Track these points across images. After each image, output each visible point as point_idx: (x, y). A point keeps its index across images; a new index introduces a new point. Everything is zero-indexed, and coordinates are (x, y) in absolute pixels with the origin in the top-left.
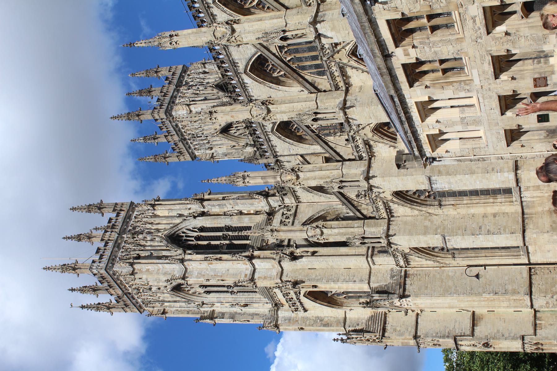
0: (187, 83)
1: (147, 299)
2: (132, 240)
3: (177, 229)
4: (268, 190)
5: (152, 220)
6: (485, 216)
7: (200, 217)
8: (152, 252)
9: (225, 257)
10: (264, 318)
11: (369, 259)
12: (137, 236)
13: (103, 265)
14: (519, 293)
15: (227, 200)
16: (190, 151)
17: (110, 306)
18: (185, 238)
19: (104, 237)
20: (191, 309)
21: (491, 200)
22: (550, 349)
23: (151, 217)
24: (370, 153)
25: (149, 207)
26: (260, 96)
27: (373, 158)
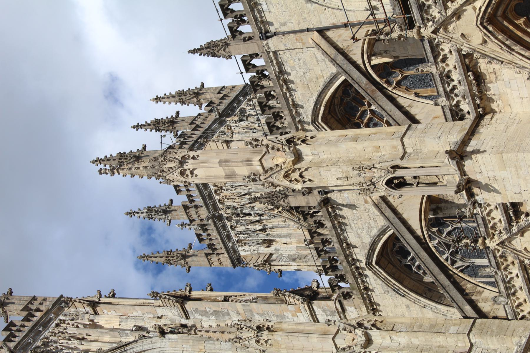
0: (243, 111)
4: (318, 287)
5: (83, 332)
15: (232, 301)
16: (230, 245)
24: (481, 99)
26: (285, 24)
27: (488, 117)
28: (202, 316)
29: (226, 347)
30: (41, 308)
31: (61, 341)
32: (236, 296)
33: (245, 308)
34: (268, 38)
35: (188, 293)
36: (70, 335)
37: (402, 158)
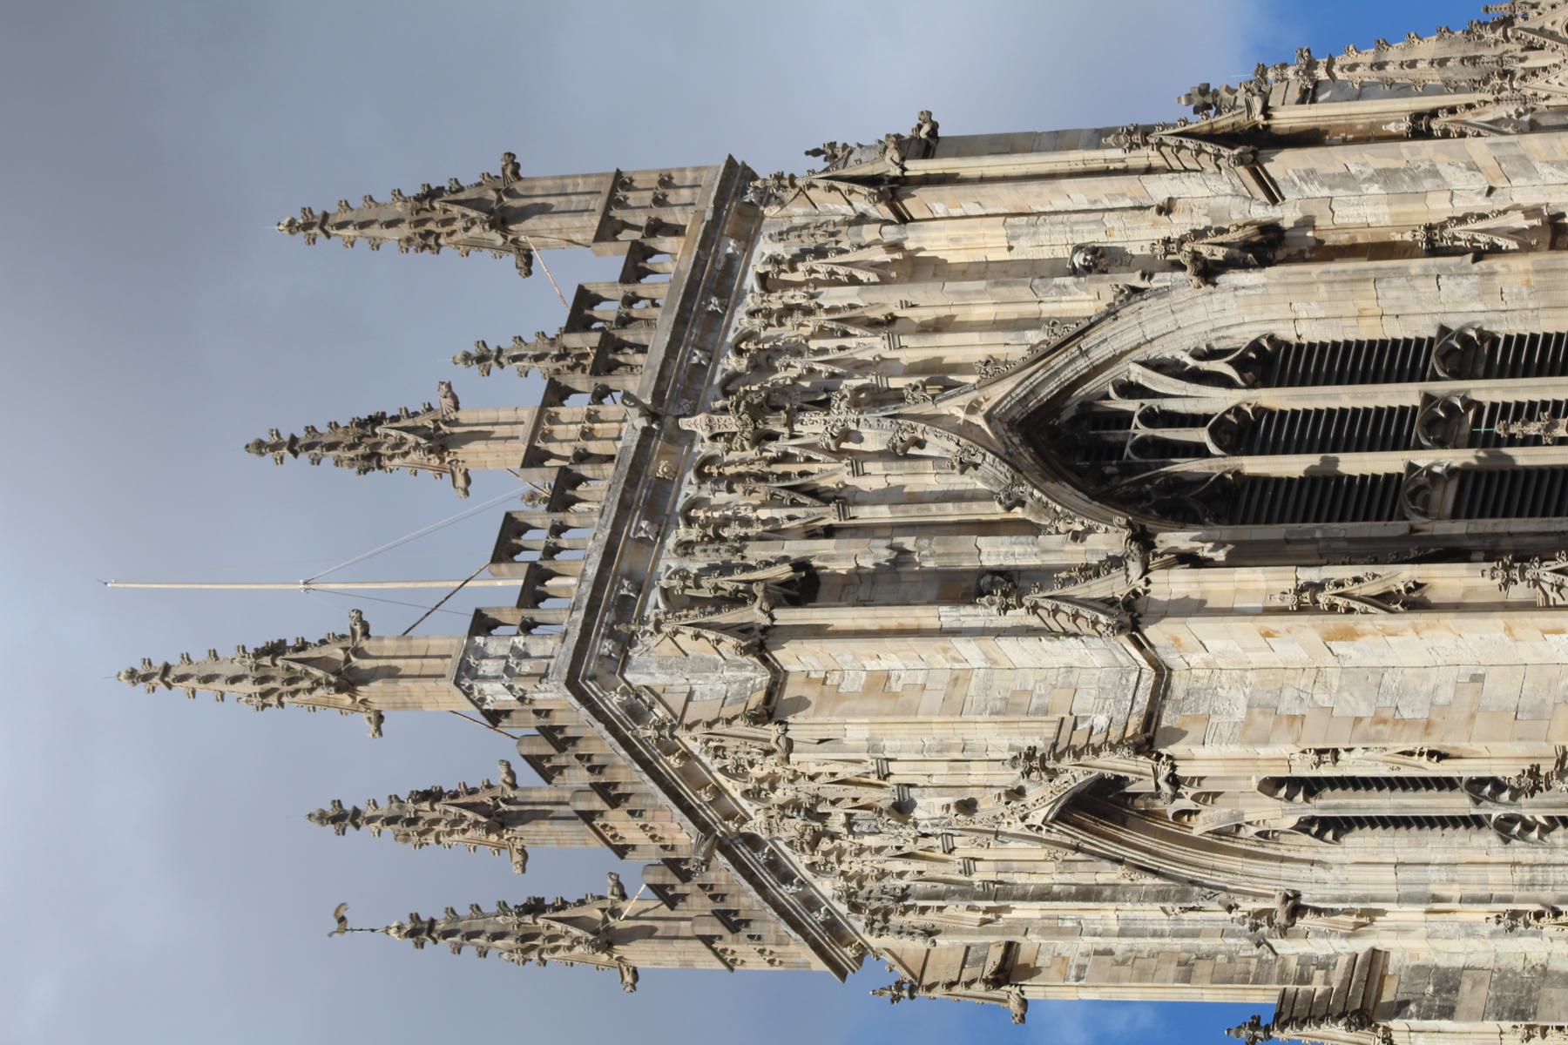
1: (883, 874)
2: (751, 453)
3: (1082, 365)
5: (888, 300)
7: (1245, 266)
8: (909, 542)
9: (1446, 579)
12: (789, 424)
13: (552, 648)
15: (1446, 134)
17: (618, 924)
18: (1142, 431)
19: (549, 437)
20: (1205, 944)
23: (884, 281)
25: (862, 202)
28: (1331, 187)
29: (1460, 292)
30: (670, 217)
31: (814, 344)
32: (1452, 110)
33: (1498, 153)
35: (1260, 119)
36: (837, 316)
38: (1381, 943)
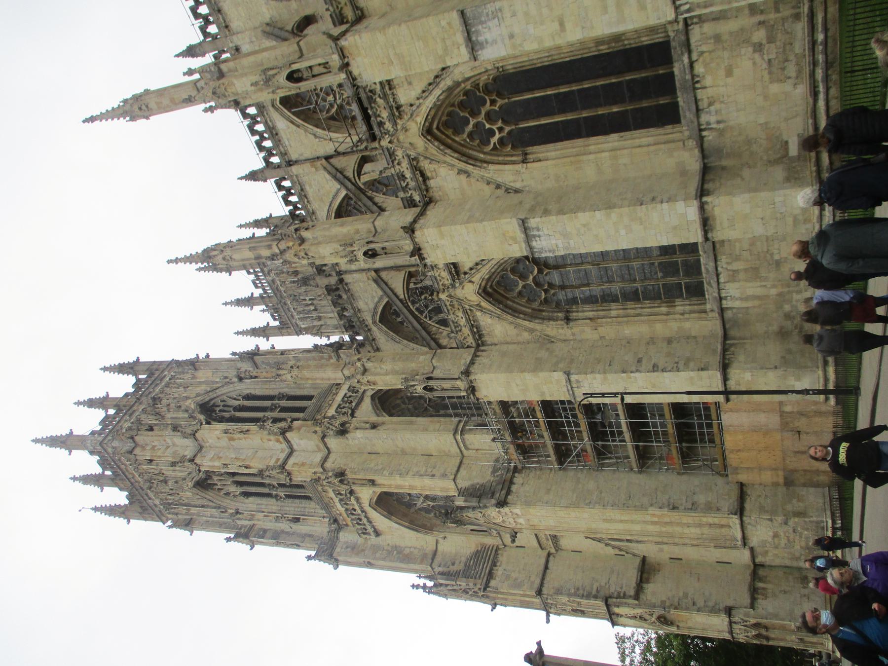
3: (215, 395)
6: (652, 341)
10: (319, 542)
11: (458, 437)
14: (718, 509)
16: (294, 321)
21: (664, 309)
22: (782, 640)
26: (302, 155)
27: (433, 204)
34: (291, 165)
37: (374, 236)
38: (255, 522)
